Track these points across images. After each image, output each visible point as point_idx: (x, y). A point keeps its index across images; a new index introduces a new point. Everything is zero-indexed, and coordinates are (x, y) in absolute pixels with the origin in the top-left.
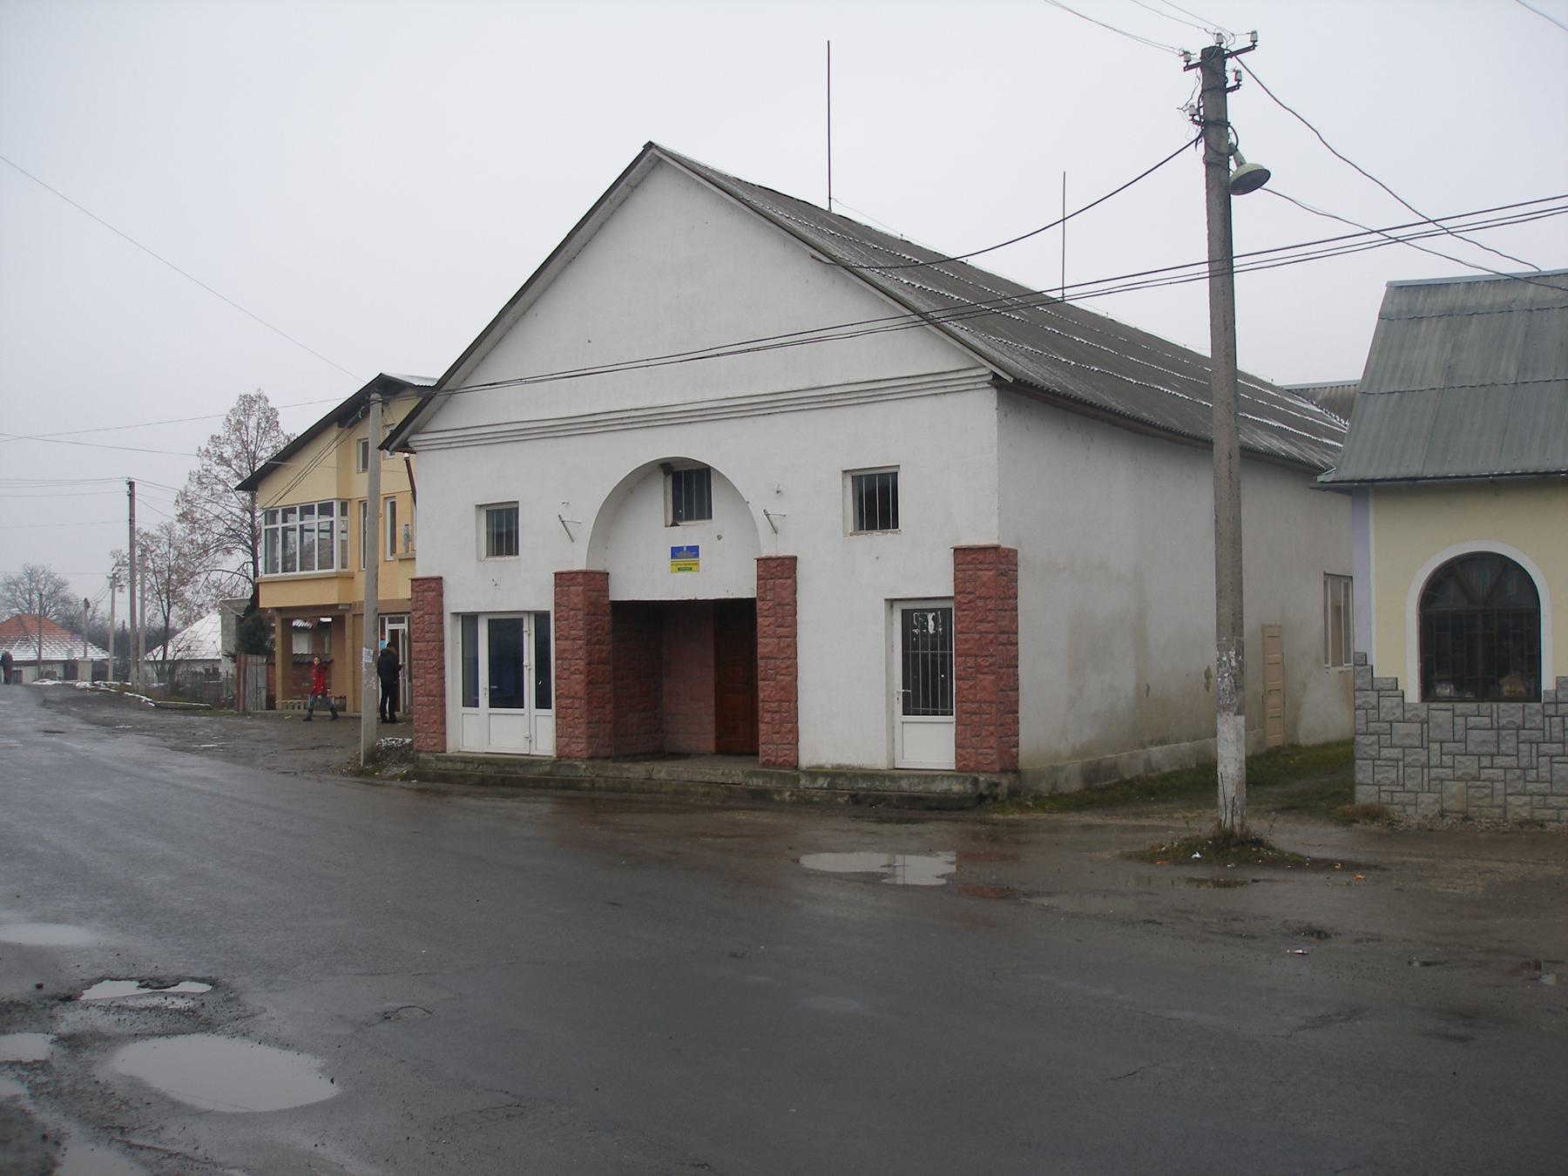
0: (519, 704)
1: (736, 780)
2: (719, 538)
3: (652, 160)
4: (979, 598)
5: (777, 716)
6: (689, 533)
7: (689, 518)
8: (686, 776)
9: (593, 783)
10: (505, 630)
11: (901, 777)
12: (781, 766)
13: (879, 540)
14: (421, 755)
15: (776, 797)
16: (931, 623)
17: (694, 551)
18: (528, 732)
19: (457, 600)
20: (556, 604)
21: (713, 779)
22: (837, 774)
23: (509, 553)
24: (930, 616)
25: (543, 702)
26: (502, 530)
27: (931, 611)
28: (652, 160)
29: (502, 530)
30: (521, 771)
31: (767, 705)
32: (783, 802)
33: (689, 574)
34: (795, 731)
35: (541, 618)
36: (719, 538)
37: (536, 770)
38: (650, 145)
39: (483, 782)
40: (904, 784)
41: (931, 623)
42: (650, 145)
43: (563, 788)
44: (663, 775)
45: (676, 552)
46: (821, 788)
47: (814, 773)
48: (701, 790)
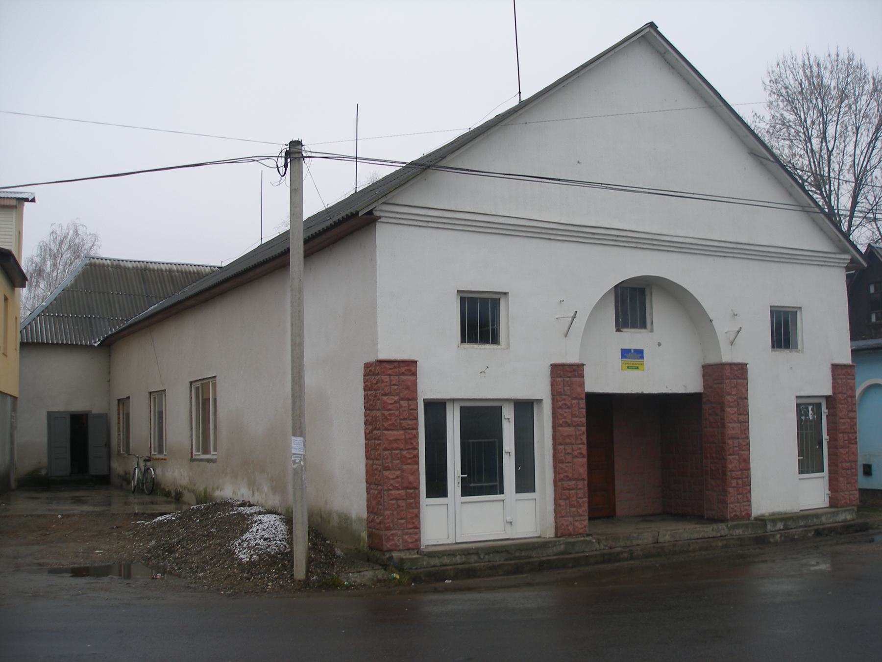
0: (497, 488)
1: (723, 533)
2: (659, 344)
3: (649, 37)
4: (849, 396)
5: (740, 481)
6: (632, 338)
7: (625, 325)
8: (685, 536)
9: (631, 553)
10: (481, 420)
11: (822, 515)
12: (743, 518)
13: (783, 355)
14: (395, 555)
15: (772, 540)
16: (810, 412)
17: (640, 353)
18: (516, 516)
19: (429, 387)
20: (556, 395)
21: (706, 535)
22: (787, 519)
23: (485, 340)
24: (810, 408)
25: (525, 483)
26: (480, 320)
27: (810, 404)
28: (649, 37)
29: (480, 320)
30: (534, 554)
31: (734, 474)
32: (776, 543)
33: (636, 371)
34: (750, 491)
35: (525, 409)
36: (659, 344)
37: (550, 551)
38: (652, 25)
39: (517, 570)
40: (824, 519)
41: (810, 412)
42: (652, 25)
43: (604, 562)
44: (667, 538)
45: (625, 353)
46: (780, 530)
47: (762, 521)
48: (720, 544)
